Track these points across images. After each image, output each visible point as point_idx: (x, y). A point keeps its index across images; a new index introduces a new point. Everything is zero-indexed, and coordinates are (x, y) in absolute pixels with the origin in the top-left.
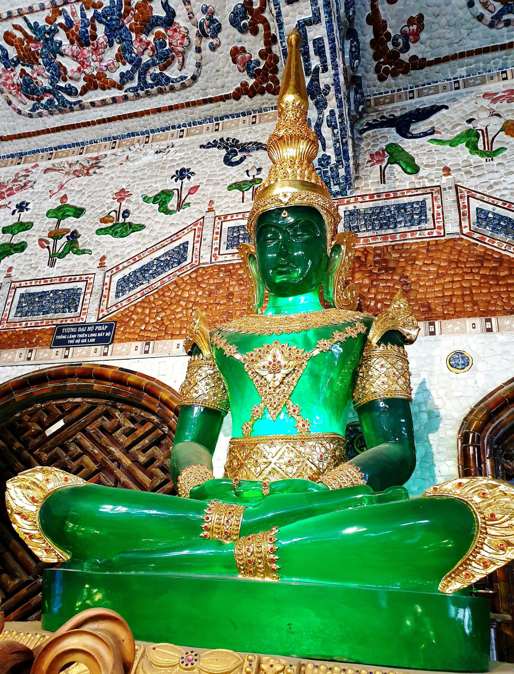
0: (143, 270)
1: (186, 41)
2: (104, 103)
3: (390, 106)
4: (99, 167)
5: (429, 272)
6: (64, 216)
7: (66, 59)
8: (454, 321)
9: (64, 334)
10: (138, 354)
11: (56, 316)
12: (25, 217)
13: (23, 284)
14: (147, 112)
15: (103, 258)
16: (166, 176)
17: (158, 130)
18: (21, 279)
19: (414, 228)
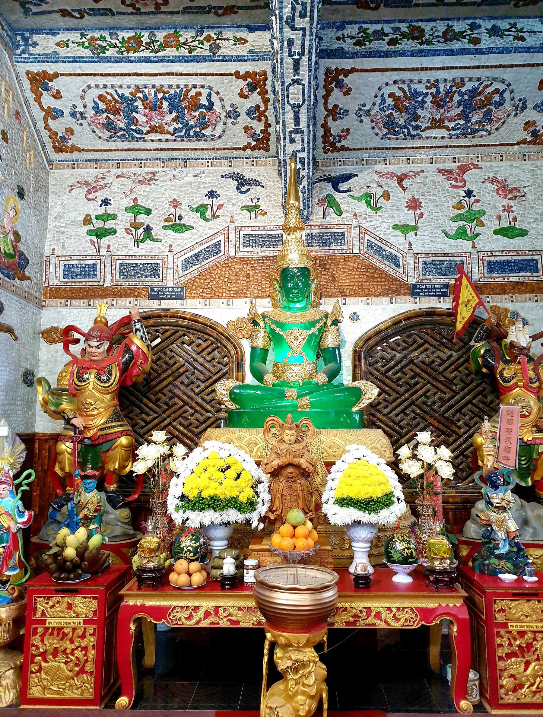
0: (197, 256)
2: (160, 141)
6: (138, 213)
8: (354, 298)
10: (201, 306)
11: (147, 280)
12: (110, 210)
15: (171, 246)
18: (119, 253)
19: (339, 248)
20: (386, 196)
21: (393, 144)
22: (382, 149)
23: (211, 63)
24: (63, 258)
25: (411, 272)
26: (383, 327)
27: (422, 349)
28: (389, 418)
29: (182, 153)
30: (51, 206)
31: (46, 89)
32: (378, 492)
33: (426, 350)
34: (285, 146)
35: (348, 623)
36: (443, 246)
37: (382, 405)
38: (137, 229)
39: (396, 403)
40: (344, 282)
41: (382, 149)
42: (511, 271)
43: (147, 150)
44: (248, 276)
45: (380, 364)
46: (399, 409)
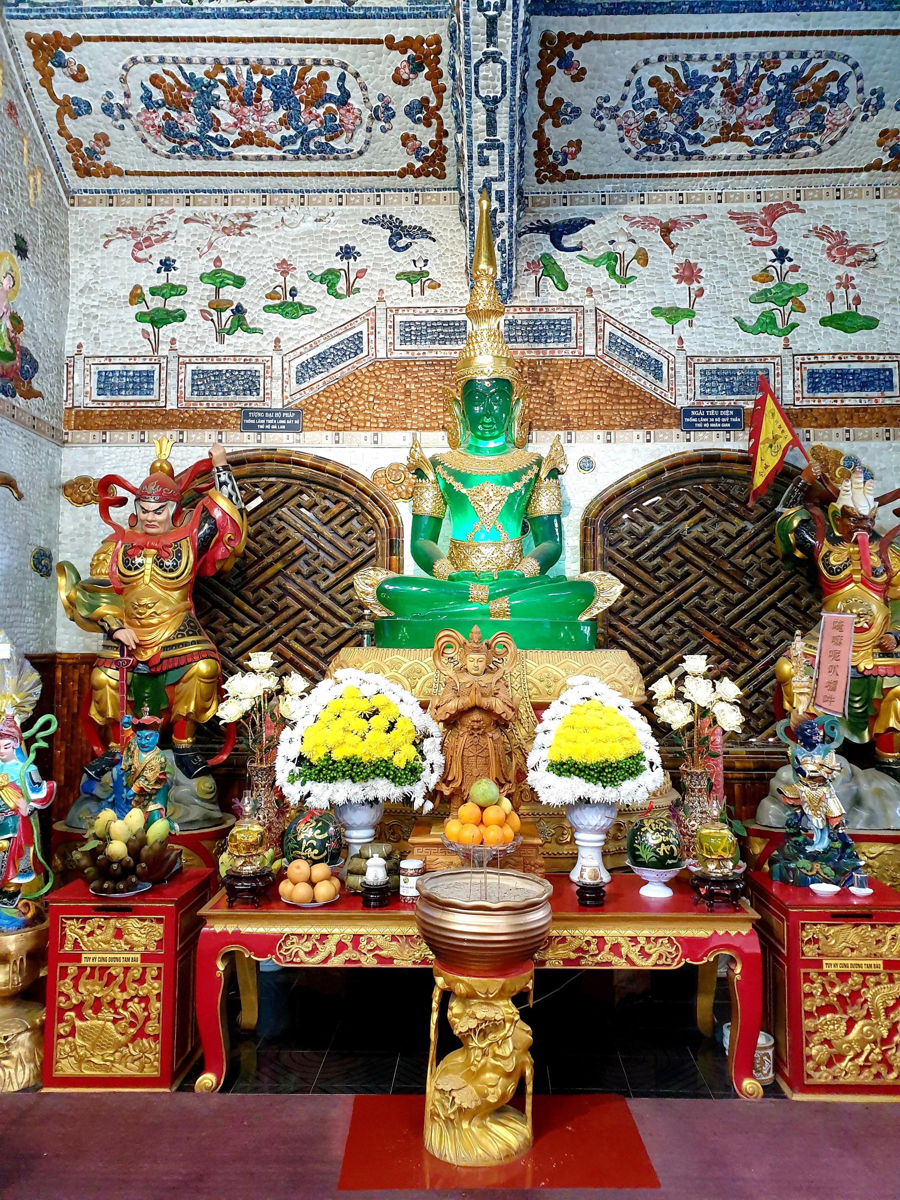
0: (322, 357)
1: (358, 121)
2: (258, 158)
3: (546, 209)
4: (252, 227)
5: (570, 388)
6: (223, 284)
7: (221, 111)
8: (585, 432)
9: (252, 418)
10: (329, 443)
11: (238, 398)
12: (175, 277)
13: (193, 360)
14: (305, 174)
16: (330, 252)
17: (314, 191)
18: (191, 352)
19: (561, 345)
20: (643, 258)
21: (655, 168)
22: (637, 176)
23: (345, 21)
24: (97, 361)
25: (682, 389)
26: (632, 481)
27: (696, 518)
28: (640, 632)
29: (297, 180)
30: (75, 271)
31: (62, 64)
32: (618, 753)
33: (703, 520)
34: (470, 171)
35: (567, 961)
36: (736, 345)
37: (627, 611)
38: (220, 311)
39: (651, 607)
40: (569, 404)
41: (637, 176)
42: (848, 388)
43: (236, 174)
44: (407, 393)
45: (627, 543)
46: (656, 617)
